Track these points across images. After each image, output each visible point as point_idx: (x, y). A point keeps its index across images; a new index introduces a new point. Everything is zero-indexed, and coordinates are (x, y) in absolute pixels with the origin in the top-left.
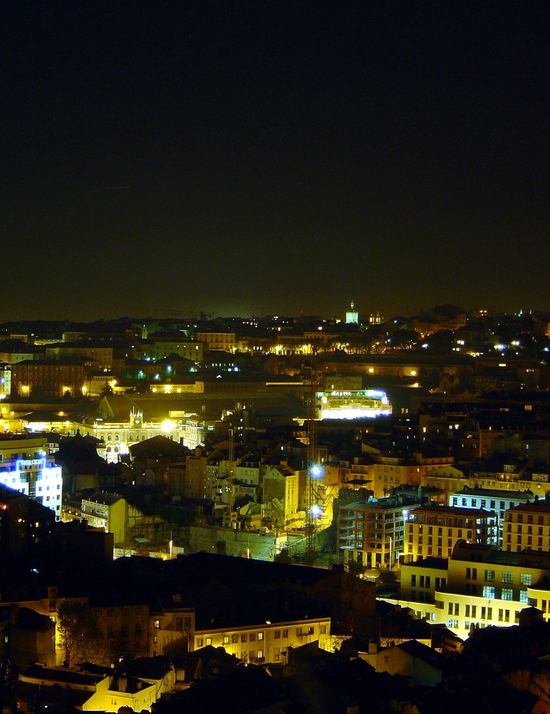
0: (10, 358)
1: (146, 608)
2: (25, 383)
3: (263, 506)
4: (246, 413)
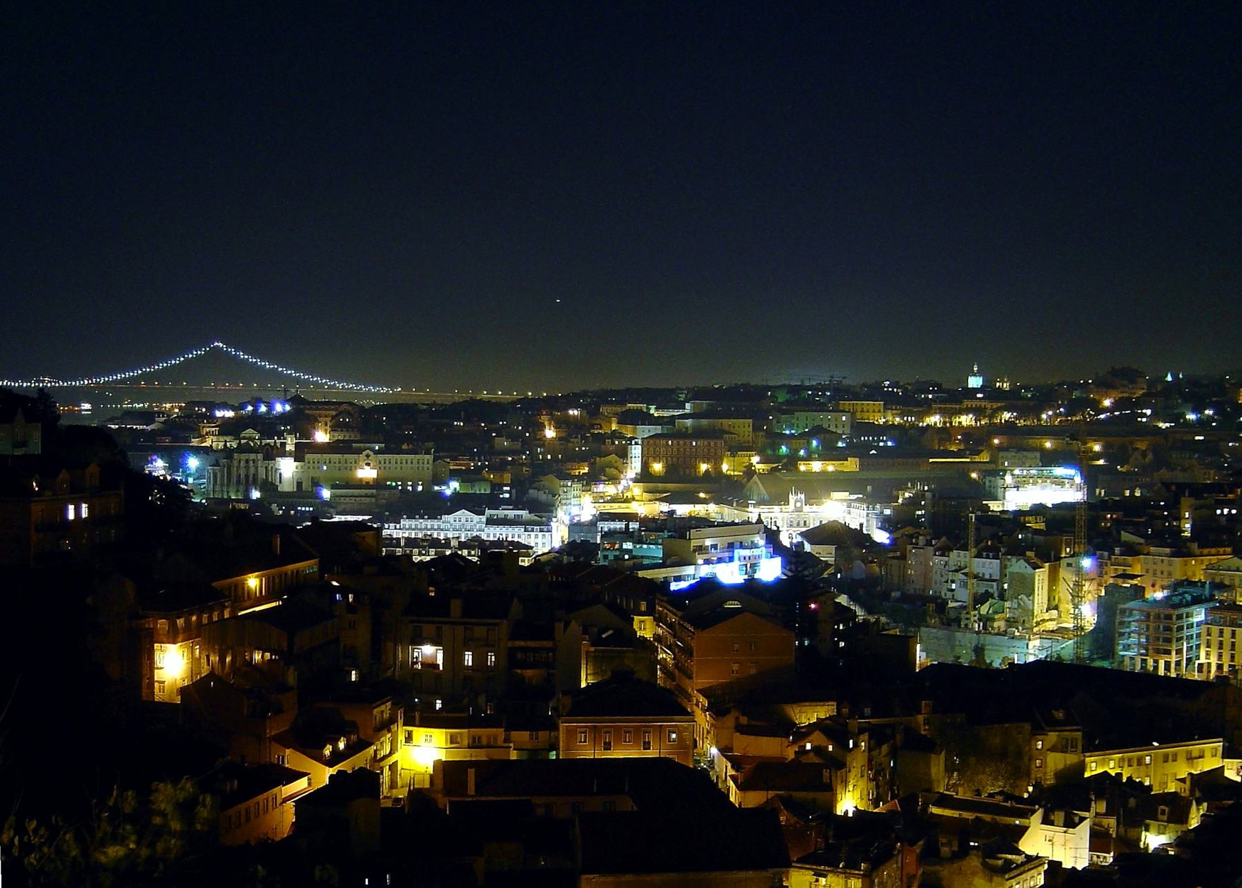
0: (634, 431)
1: (1027, 727)
2: (657, 458)
3: (1007, 604)
4: (928, 495)
